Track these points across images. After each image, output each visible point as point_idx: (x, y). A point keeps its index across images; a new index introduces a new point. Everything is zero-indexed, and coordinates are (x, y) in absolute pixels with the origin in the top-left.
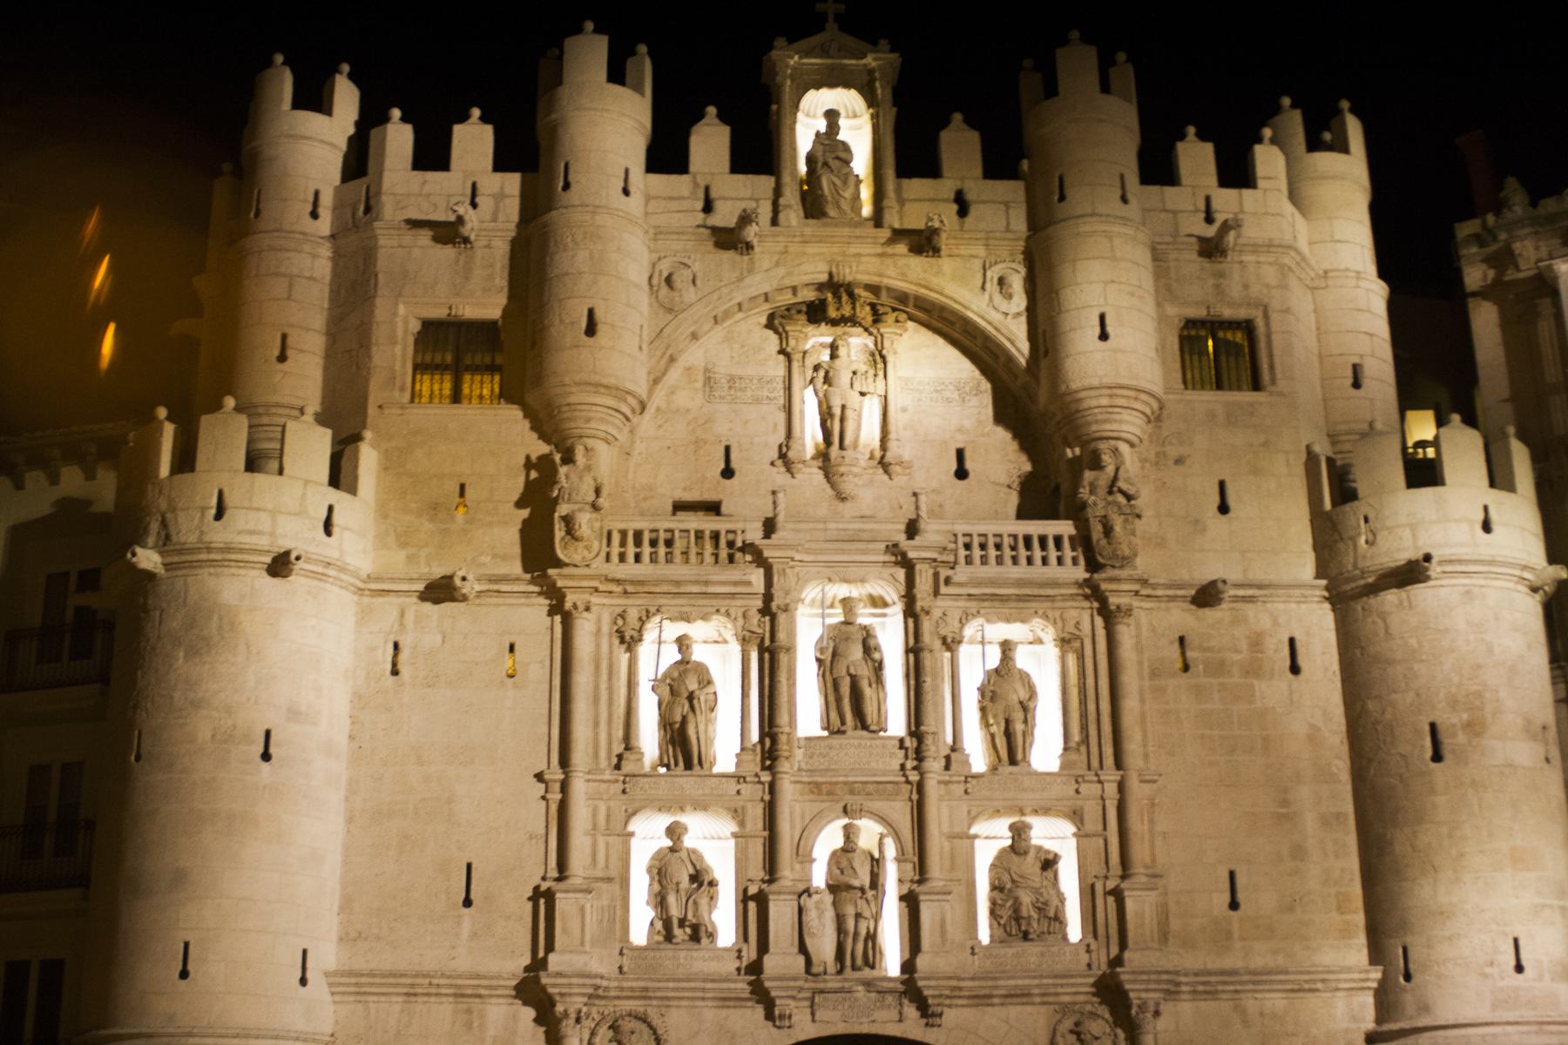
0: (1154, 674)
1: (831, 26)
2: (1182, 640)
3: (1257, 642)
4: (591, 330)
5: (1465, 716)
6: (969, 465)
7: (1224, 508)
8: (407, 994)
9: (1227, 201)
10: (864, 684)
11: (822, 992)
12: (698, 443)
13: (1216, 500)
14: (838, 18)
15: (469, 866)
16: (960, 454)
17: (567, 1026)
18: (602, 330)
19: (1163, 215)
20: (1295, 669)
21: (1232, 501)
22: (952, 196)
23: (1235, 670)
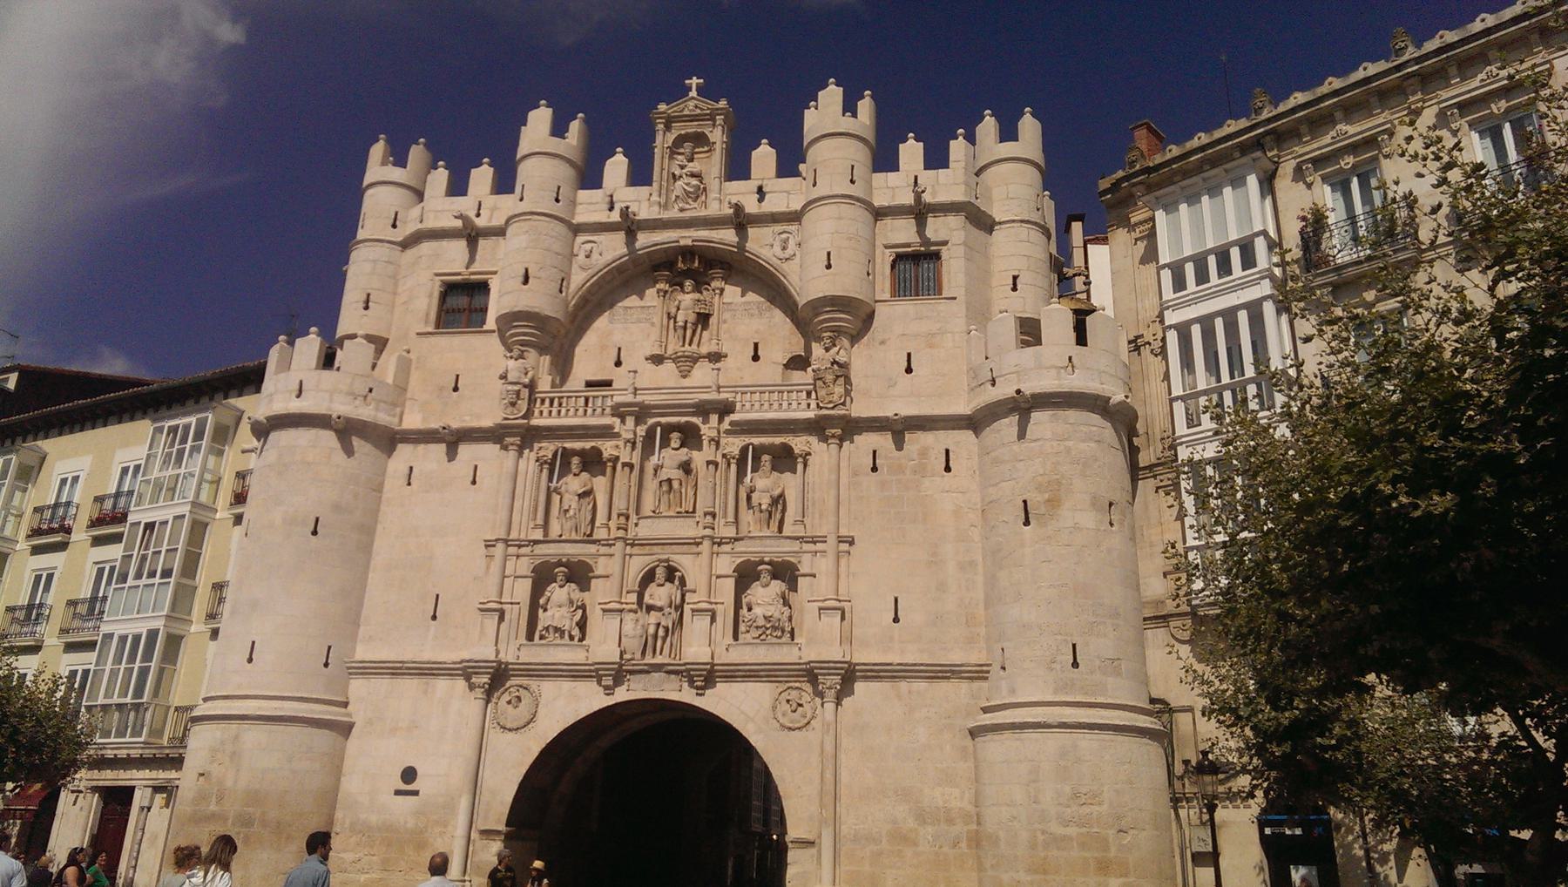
0: (856, 474)
1: (693, 93)
2: (875, 452)
3: (924, 453)
4: (526, 280)
5: (1046, 496)
6: (760, 353)
7: (909, 370)
8: (393, 674)
9: (928, 176)
10: (676, 485)
11: (632, 672)
12: (603, 347)
13: (906, 364)
14: (699, 89)
15: (438, 596)
16: (756, 345)
18: (530, 281)
19: (886, 191)
20: (948, 469)
21: (913, 366)
22: (756, 190)
23: (908, 472)
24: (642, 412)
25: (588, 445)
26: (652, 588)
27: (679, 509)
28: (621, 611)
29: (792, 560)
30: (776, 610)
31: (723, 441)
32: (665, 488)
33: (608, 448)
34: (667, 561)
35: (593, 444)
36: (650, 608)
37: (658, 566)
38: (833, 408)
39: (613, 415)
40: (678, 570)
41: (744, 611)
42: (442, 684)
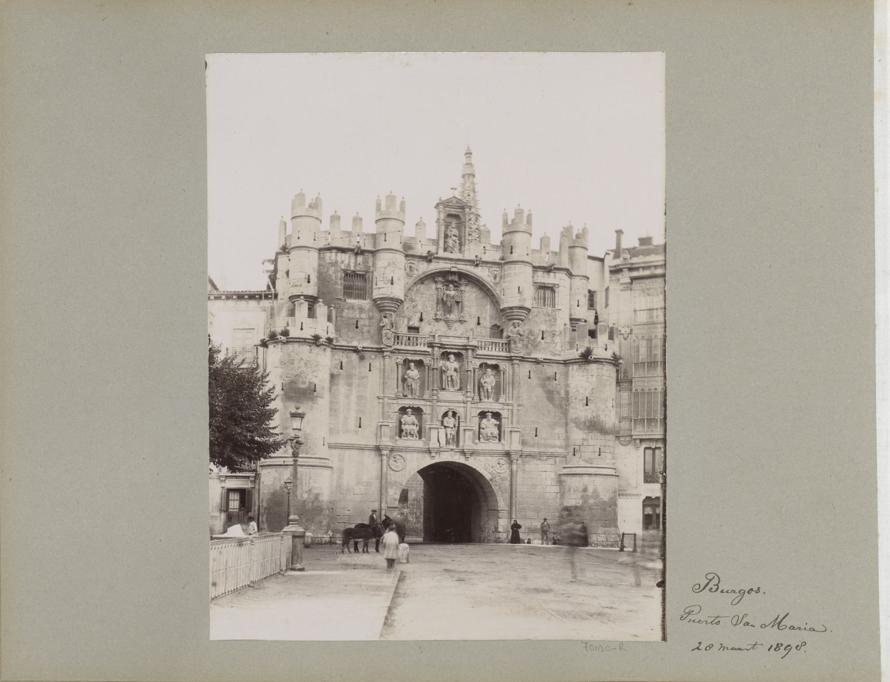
16: (479, 318)
17: (384, 458)
24: (442, 346)
25: (417, 358)
26: (446, 419)
27: (456, 389)
28: (438, 428)
29: (500, 412)
30: (496, 432)
31: (473, 362)
32: (450, 379)
33: (427, 360)
34: (453, 409)
35: (421, 358)
36: (445, 427)
37: (449, 411)
38: (517, 353)
39: (429, 347)
40: (457, 413)
41: (481, 430)
42: (367, 452)
